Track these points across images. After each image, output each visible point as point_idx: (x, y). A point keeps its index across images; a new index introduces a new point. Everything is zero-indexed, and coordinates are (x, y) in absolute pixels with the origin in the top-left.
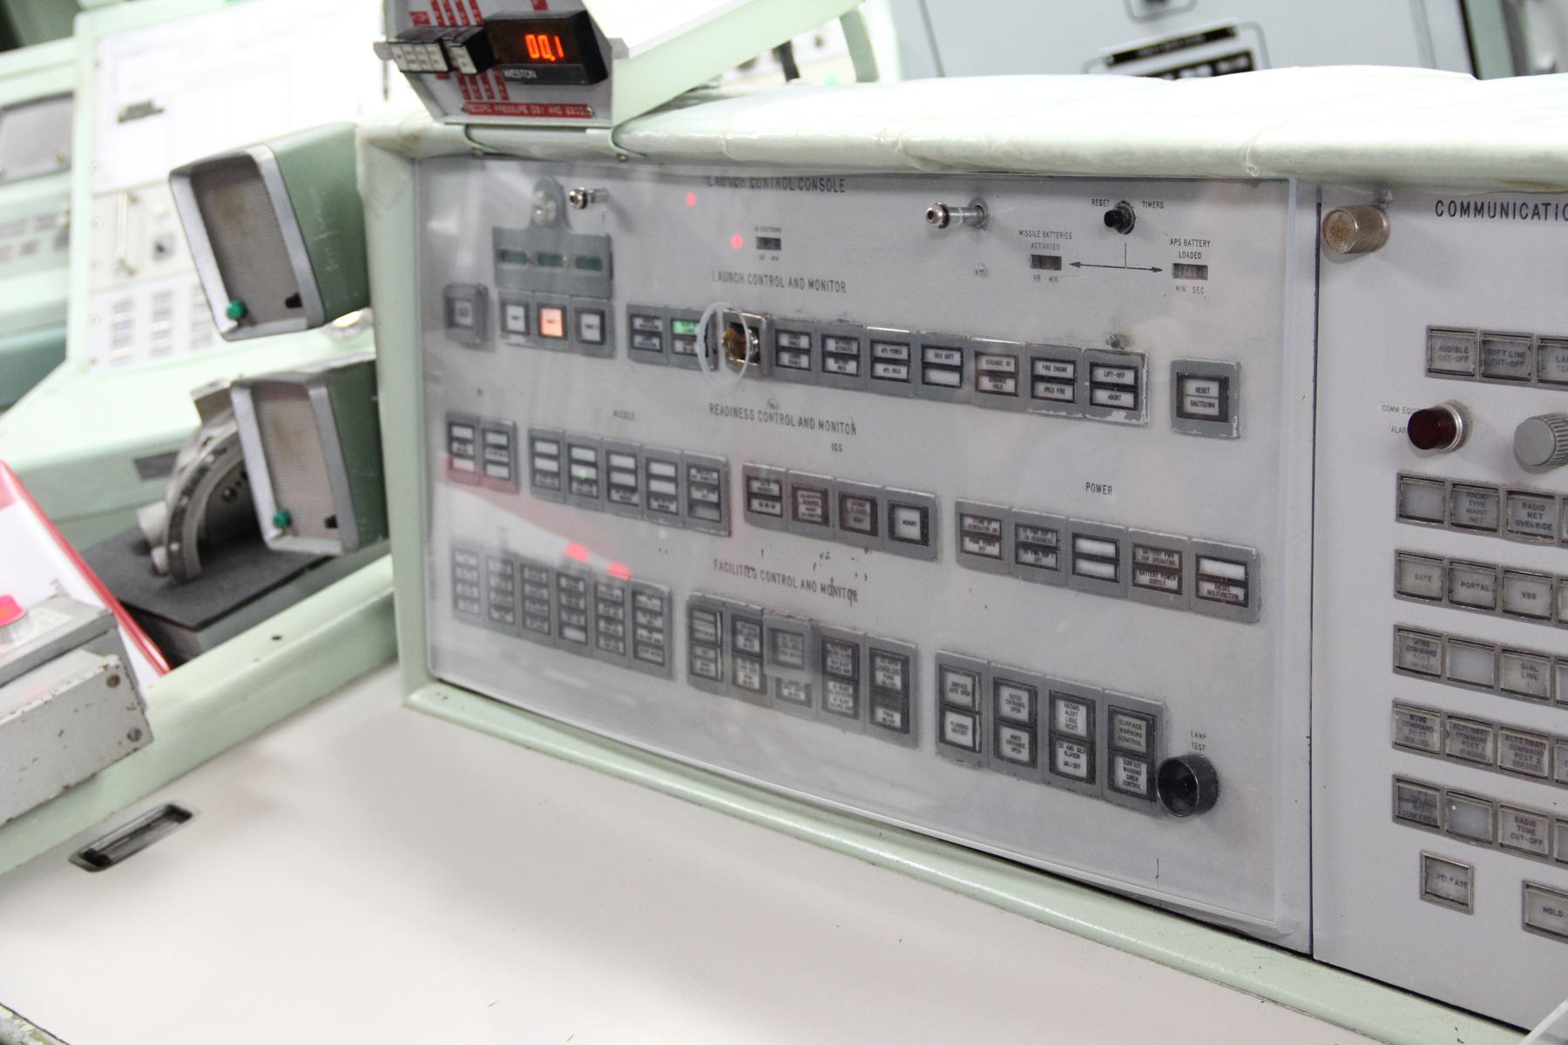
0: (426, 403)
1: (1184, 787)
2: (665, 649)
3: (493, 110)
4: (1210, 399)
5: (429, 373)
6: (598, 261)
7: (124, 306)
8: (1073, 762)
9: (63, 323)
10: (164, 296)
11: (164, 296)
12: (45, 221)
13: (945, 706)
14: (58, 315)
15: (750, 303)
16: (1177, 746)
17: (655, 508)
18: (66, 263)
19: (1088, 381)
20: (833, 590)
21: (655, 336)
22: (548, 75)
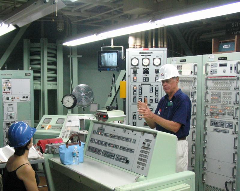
0: (90, 137)
1: (127, 162)
2: (101, 153)
3: (100, 120)
4: (134, 142)
5: (91, 136)
6: (104, 130)
7: (64, 134)
8: (122, 160)
9: (59, 135)
10: (67, 134)
11: (67, 134)
12: (60, 127)
13: (116, 157)
14: (59, 134)
15: (112, 133)
16: (128, 159)
17: (103, 145)
18: (61, 130)
19: (128, 140)
20: (112, 150)
21: (106, 135)
22: (104, 118)
